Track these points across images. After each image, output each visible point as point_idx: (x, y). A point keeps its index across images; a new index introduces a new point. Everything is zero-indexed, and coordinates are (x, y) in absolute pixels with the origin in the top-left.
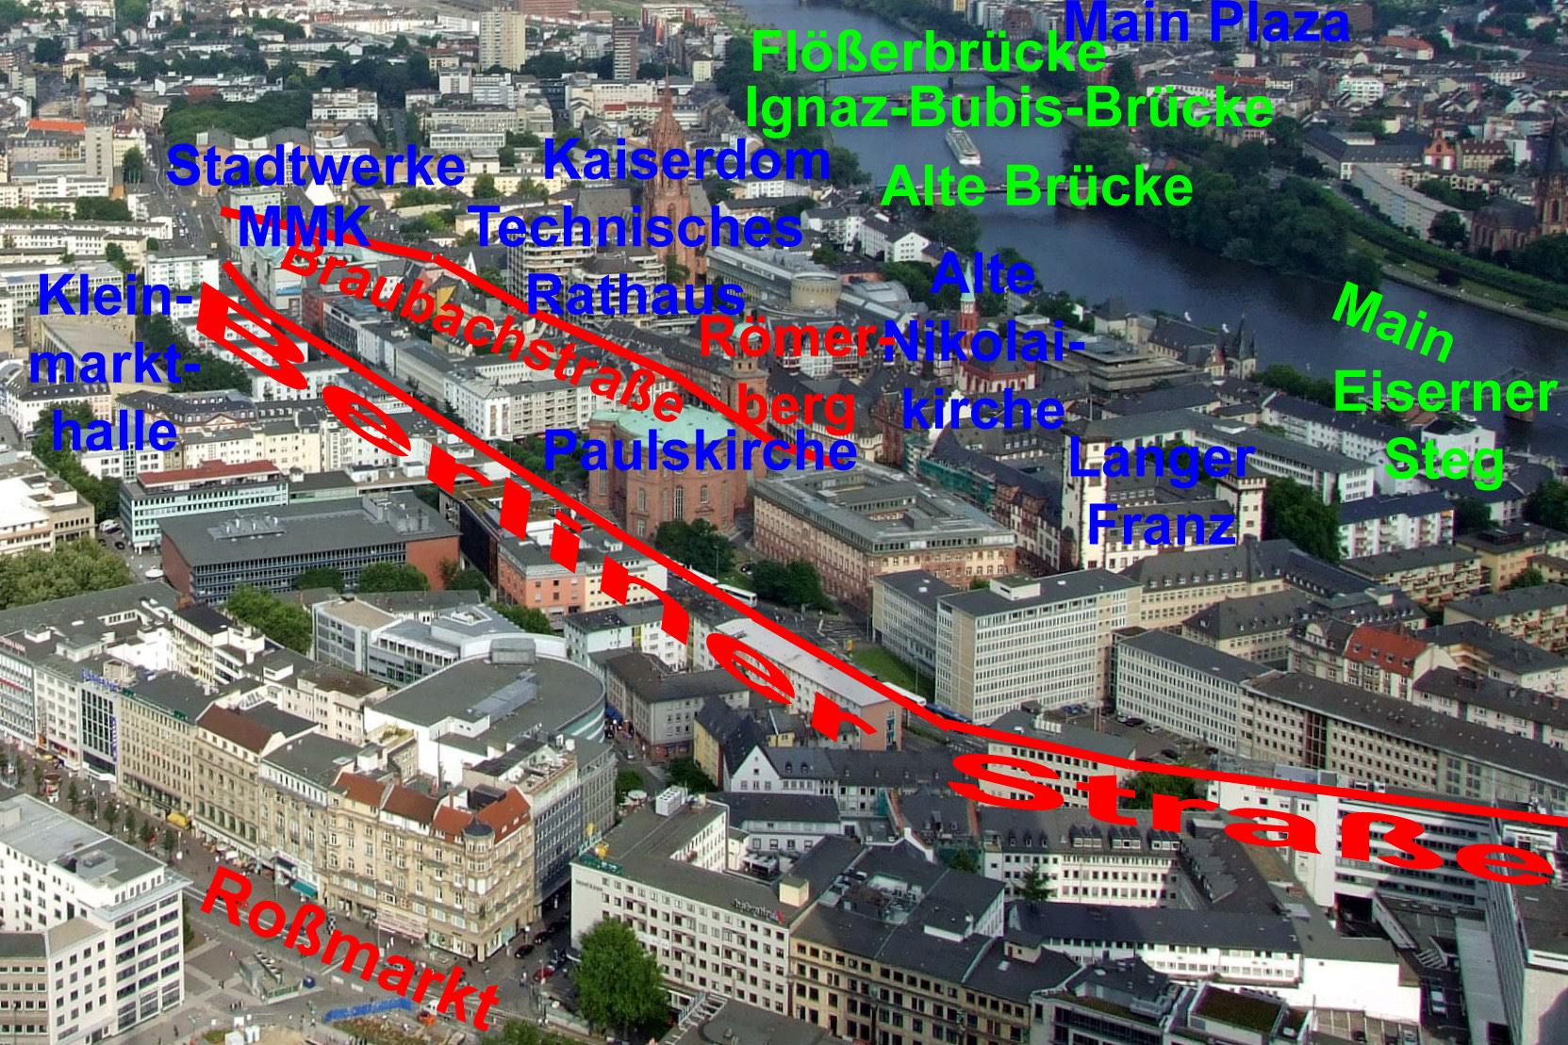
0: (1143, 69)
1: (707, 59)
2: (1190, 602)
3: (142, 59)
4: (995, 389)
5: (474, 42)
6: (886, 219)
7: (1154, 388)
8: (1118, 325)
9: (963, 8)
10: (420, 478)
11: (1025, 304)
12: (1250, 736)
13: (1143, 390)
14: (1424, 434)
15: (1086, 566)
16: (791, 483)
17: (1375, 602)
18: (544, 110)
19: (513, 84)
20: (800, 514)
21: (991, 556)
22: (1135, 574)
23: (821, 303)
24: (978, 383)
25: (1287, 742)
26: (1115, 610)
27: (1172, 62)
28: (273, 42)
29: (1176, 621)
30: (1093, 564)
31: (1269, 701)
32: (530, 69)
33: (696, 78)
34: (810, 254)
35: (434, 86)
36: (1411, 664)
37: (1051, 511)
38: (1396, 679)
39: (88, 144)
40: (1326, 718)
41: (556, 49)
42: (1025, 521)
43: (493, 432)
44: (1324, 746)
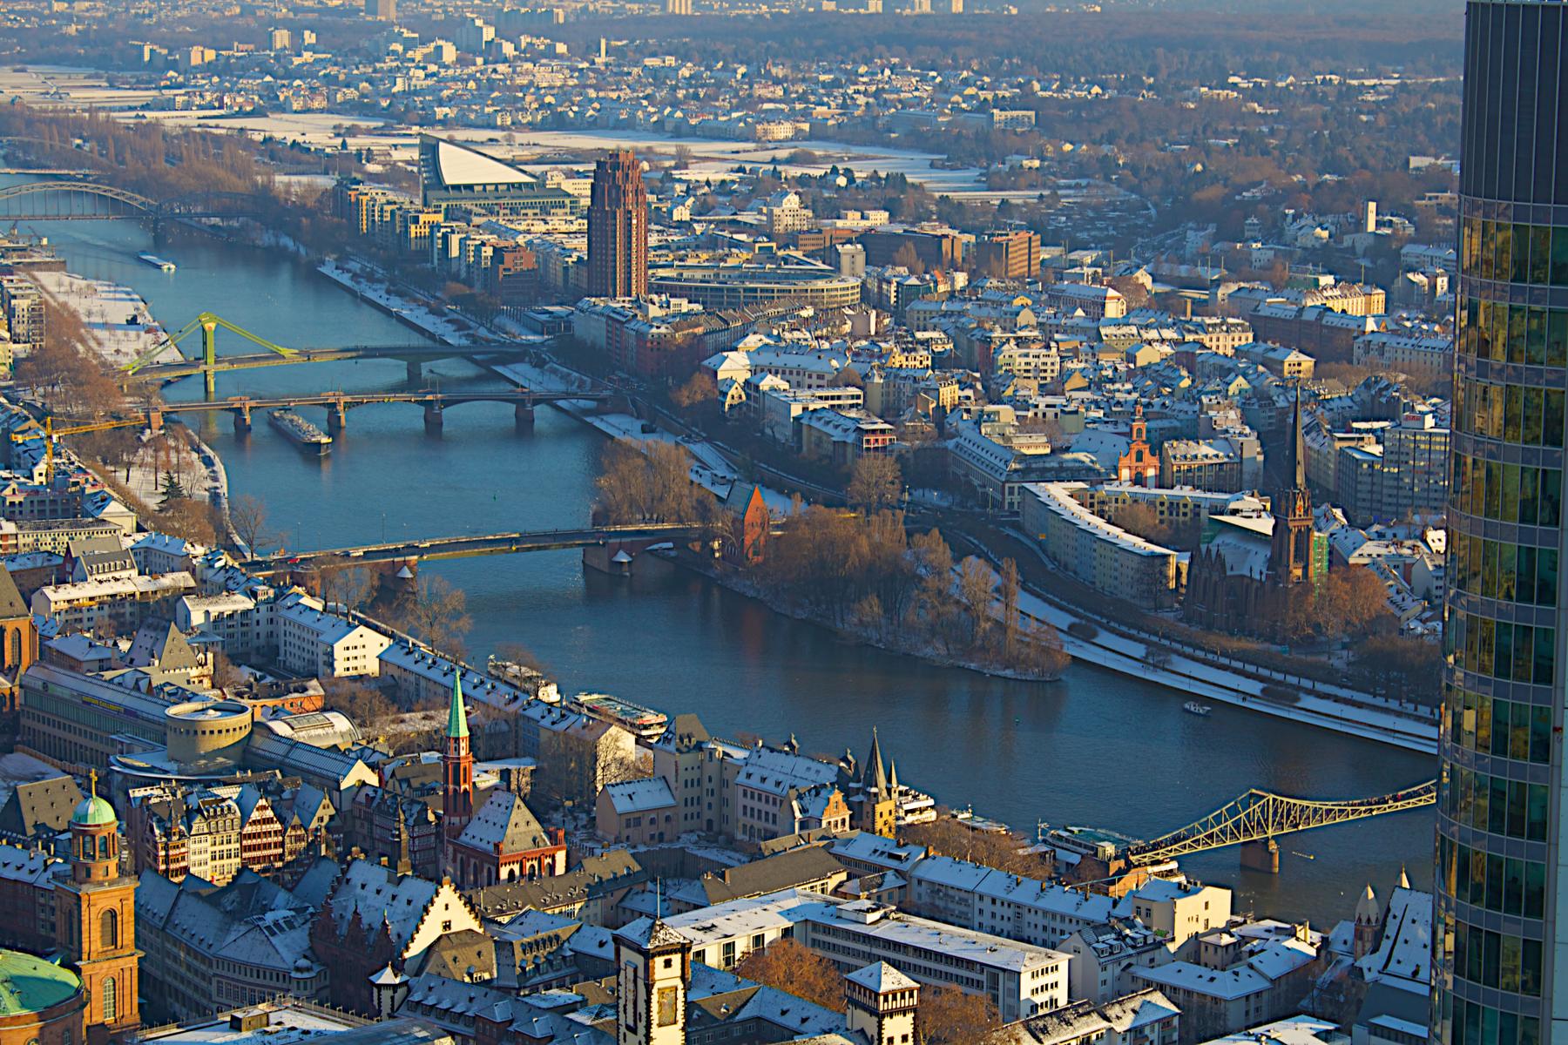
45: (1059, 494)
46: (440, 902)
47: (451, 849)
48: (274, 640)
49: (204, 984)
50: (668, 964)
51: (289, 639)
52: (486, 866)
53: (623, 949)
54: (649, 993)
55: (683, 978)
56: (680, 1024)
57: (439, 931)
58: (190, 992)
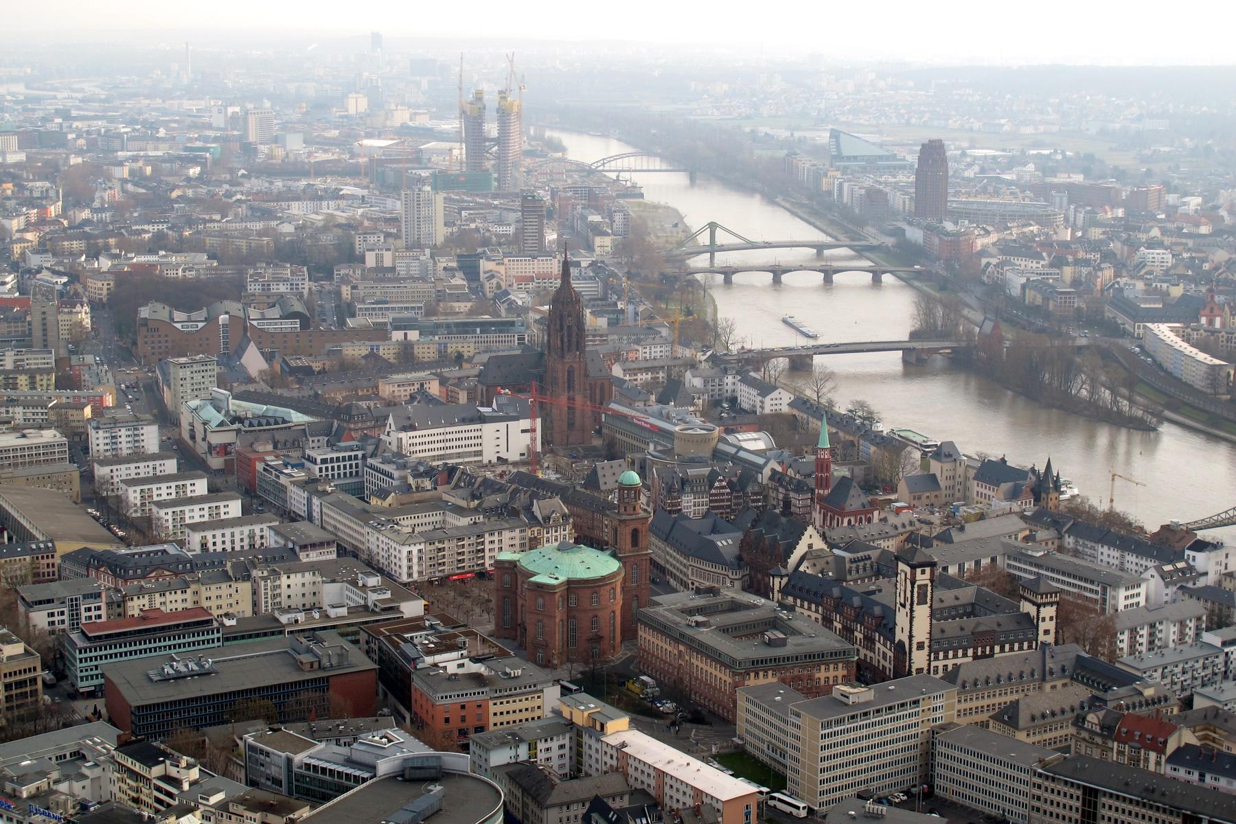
1: (608, 235)
2: (997, 700)
3: (86, 237)
4: (845, 524)
5: (394, 221)
10: (343, 618)
12: (1038, 810)
14: (1187, 552)
15: (914, 673)
16: (670, 610)
17: (1141, 694)
18: (459, 280)
19: (432, 257)
20: (679, 638)
21: (836, 669)
22: (951, 676)
24: (832, 519)
25: (1067, 813)
26: (935, 709)
28: (212, 221)
29: (984, 717)
30: (919, 671)
31: (1053, 779)
32: (450, 241)
33: (598, 251)
35: (362, 259)
36: (1165, 743)
37: (886, 626)
38: (1153, 756)
39: (34, 318)
40: (1097, 791)
41: (473, 226)
42: (865, 637)
43: (410, 575)
44: (1095, 814)
45: (1164, 331)
46: (807, 534)
48: (735, 394)
49: (685, 570)
50: (923, 572)
53: (900, 564)
54: (913, 587)
55: (932, 581)
56: (929, 604)
57: (806, 549)
58: (678, 574)
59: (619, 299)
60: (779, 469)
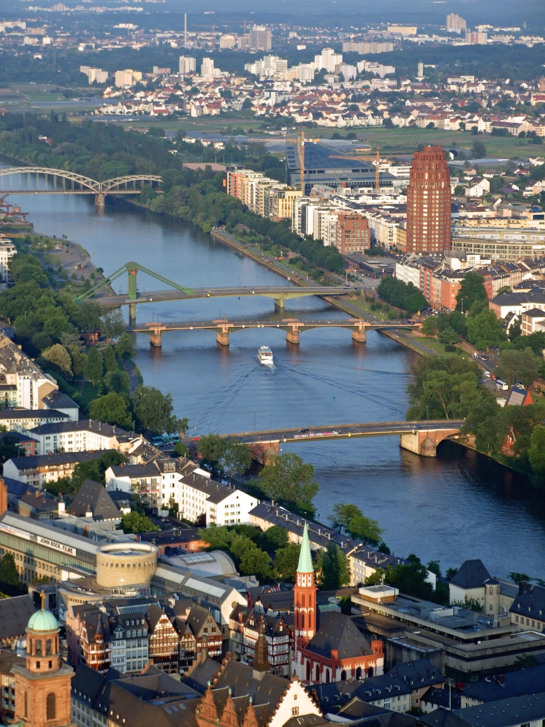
0: (497, 285)
6: (207, 475)
7: (517, 666)
8: (476, 593)
9: (289, 214)
11: (370, 571)
13: (506, 669)
23: (133, 582)
24: (319, 671)
27: (528, 276)
34: (118, 520)
47: (300, 654)
51: (186, 499)
52: (325, 668)
59: (8, 372)
60: (244, 602)
